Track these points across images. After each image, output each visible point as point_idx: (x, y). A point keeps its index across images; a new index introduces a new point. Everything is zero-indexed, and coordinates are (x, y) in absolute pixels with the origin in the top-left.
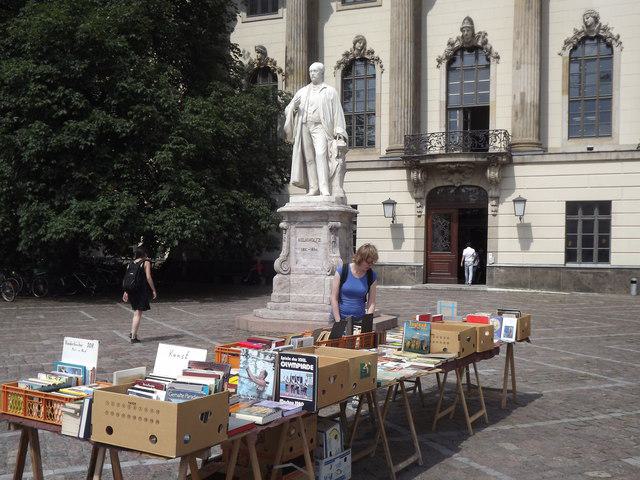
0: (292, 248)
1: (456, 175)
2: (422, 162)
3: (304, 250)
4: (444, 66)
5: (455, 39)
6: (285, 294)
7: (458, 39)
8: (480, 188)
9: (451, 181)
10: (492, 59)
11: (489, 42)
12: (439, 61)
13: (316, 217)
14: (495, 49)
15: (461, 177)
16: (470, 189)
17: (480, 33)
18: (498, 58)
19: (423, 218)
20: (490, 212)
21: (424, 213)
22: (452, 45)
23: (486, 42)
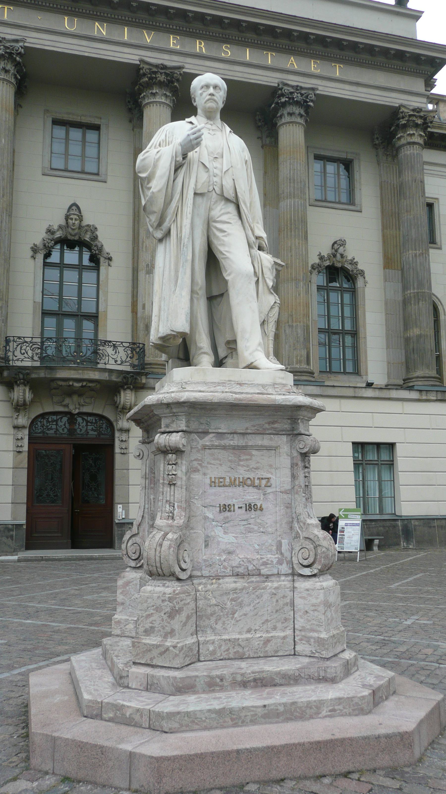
0: (198, 503)
1: (75, 398)
2: (34, 376)
3: (225, 508)
4: (40, 257)
5: (56, 227)
6: (190, 640)
7: (60, 227)
8: (101, 417)
9: (67, 406)
10: (102, 260)
11: (100, 239)
12: (35, 250)
13: (262, 421)
14: (107, 248)
15: (82, 401)
16: (89, 418)
17: (88, 226)
18: (110, 259)
19: (25, 456)
20: (117, 450)
21: (26, 448)
22: (53, 233)
23: (95, 238)
